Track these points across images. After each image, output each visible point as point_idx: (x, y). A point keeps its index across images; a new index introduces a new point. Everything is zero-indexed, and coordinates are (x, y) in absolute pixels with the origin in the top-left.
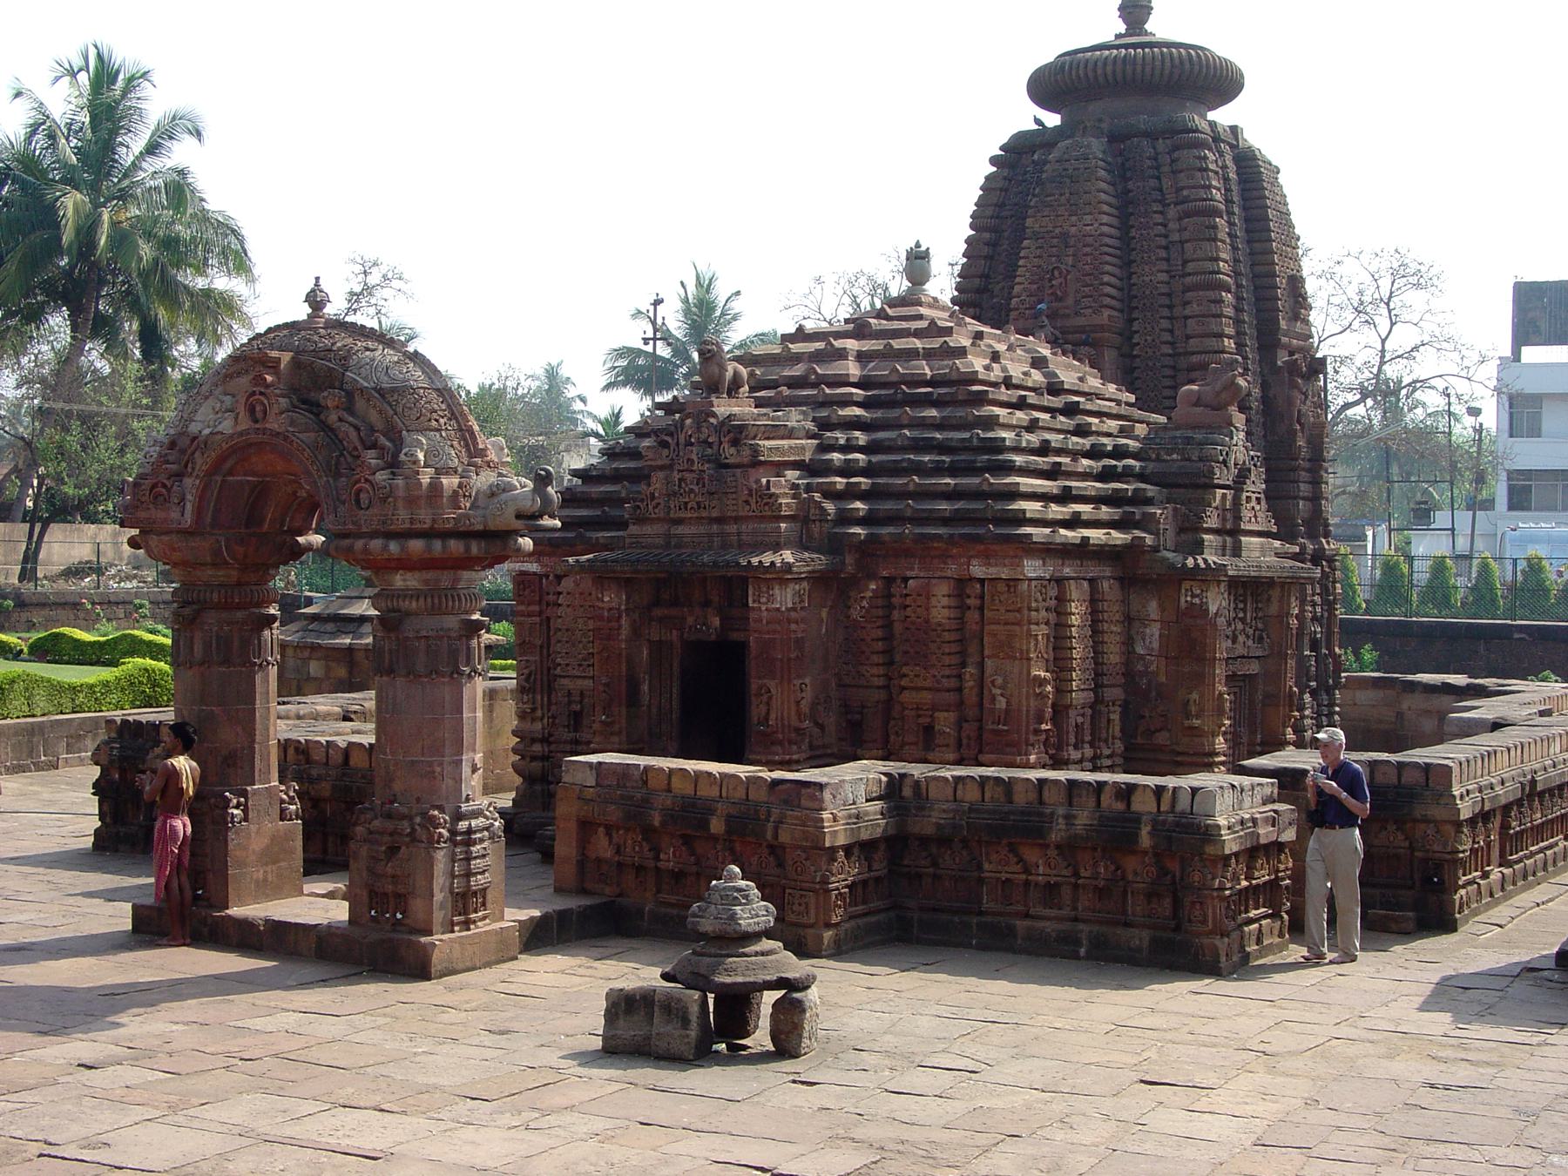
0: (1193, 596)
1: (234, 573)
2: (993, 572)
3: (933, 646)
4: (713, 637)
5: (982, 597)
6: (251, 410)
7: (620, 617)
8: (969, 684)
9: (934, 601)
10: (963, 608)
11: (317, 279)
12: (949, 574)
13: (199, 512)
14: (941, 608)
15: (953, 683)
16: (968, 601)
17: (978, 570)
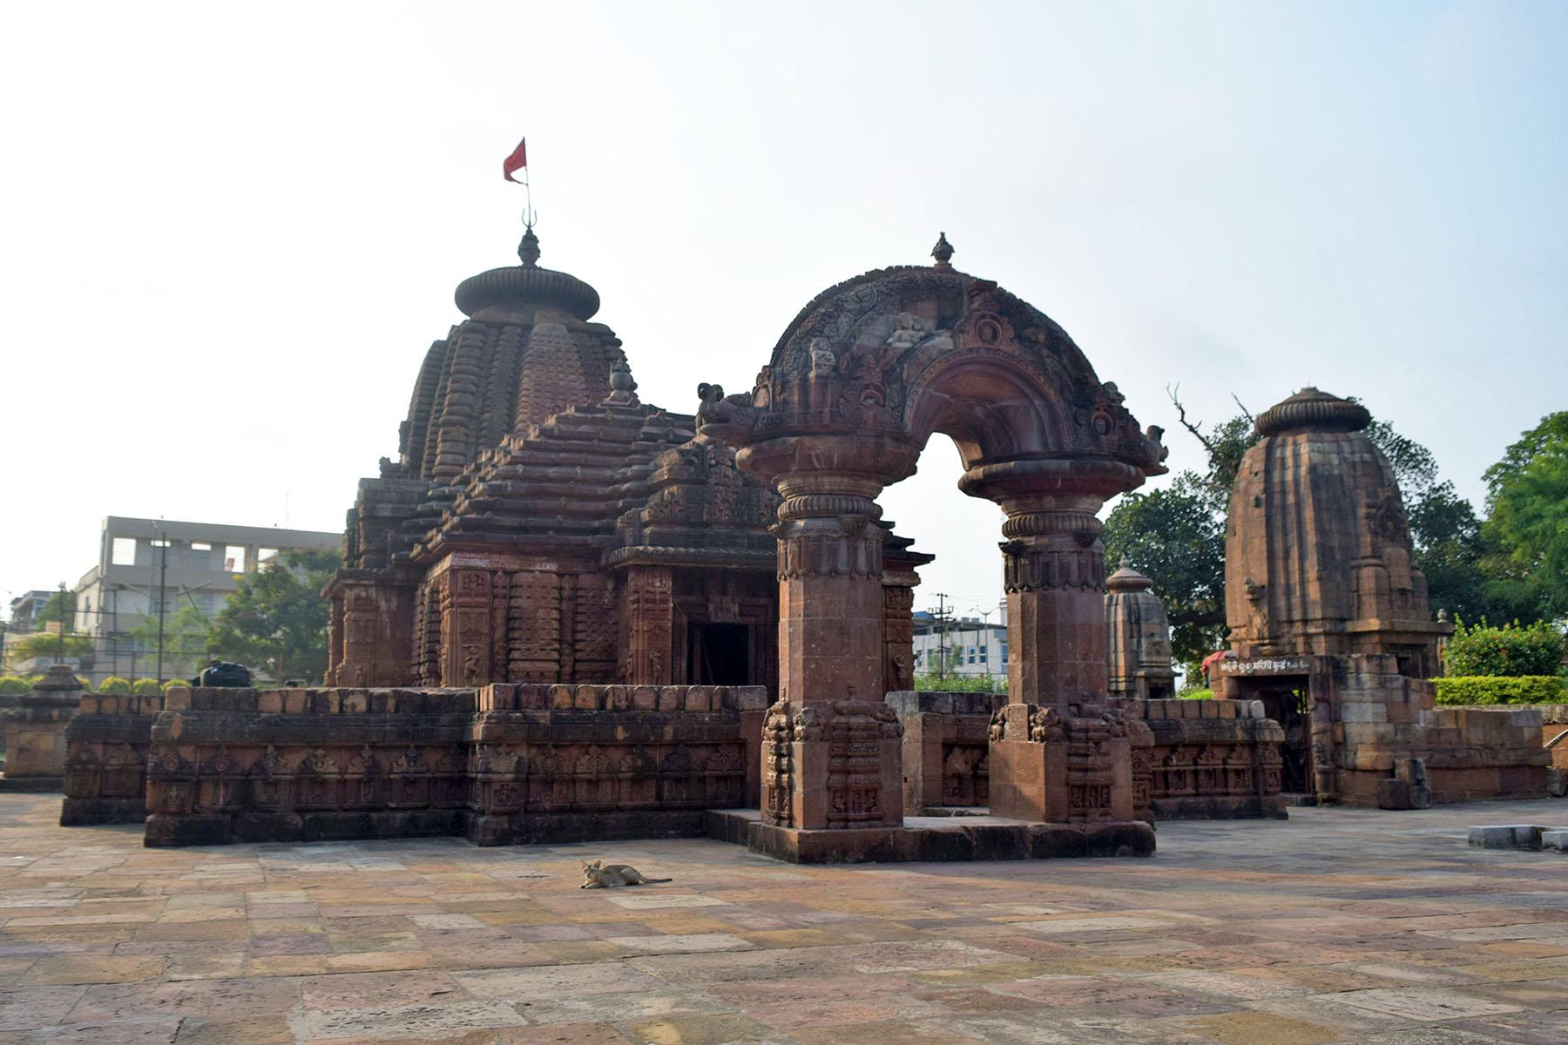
4: (738, 620)
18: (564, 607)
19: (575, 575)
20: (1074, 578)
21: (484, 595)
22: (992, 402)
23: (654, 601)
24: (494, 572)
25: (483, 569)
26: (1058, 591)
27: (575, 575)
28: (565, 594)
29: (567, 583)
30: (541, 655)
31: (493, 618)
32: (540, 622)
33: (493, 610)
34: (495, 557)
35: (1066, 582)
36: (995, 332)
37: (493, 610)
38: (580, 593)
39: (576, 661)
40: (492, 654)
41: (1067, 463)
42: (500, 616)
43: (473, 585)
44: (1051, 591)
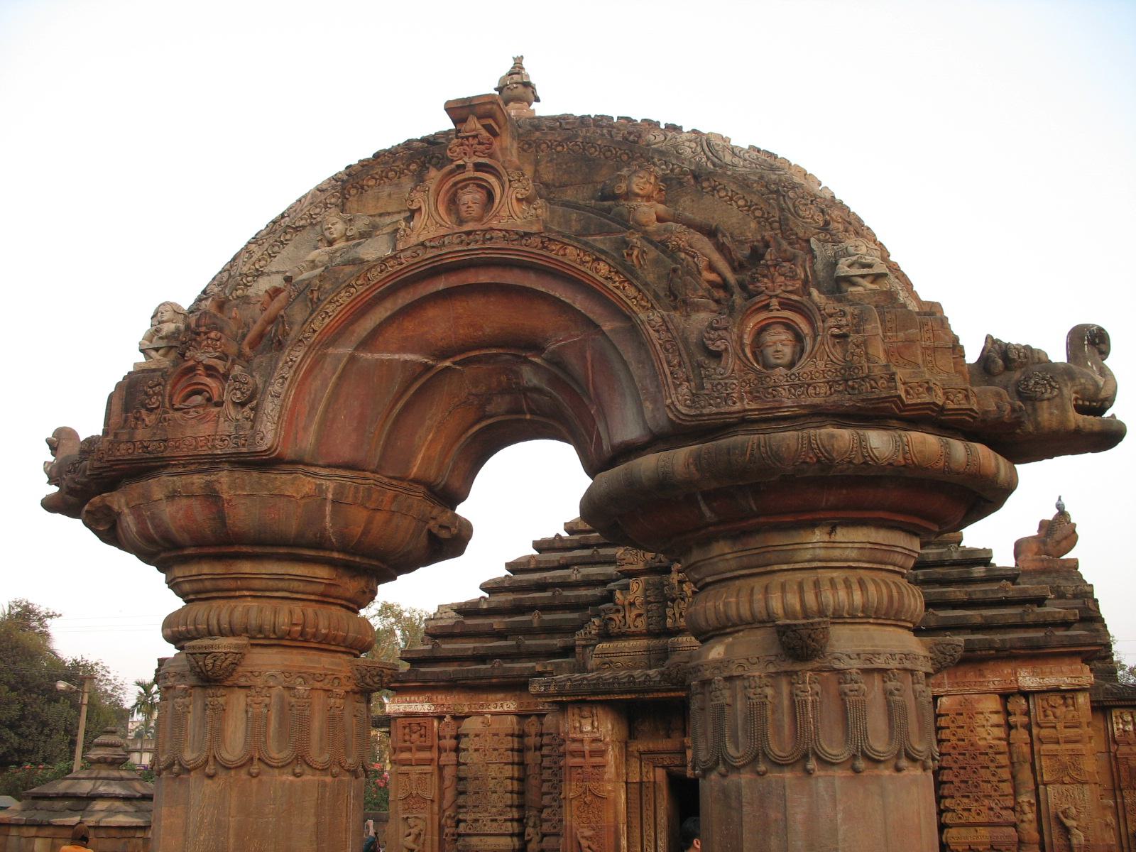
0: (1125, 723)
1: (322, 572)
2: (1051, 681)
3: (985, 774)
5: (1027, 713)
6: (453, 203)
7: (602, 753)
8: (1031, 816)
9: (980, 719)
10: (1010, 727)
11: (518, 62)
12: (992, 686)
13: (289, 420)
14: (988, 729)
15: (1008, 816)
16: (1012, 719)
17: (1027, 679)
18: (531, 757)
19: (541, 716)
20: (779, 747)
21: (430, 748)
22: (537, 348)
23: (582, 754)
24: (440, 718)
25: (425, 715)
26: (745, 778)
27: (541, 716)
28: (531, 741)
29: (532, 726)
30: (493, 827)
31: (441, 778)
32: (492, 783)
33: (441, 768)
34: (441, 698)
35: (758, 757)
36: (490, 196)
37: (441, 768)
38: (546, 740)
39: (544, 835)
40: (441, 828)
41: (680, 458)
42: (449, 772)
43: (415, 737)
44: (733, 777)
